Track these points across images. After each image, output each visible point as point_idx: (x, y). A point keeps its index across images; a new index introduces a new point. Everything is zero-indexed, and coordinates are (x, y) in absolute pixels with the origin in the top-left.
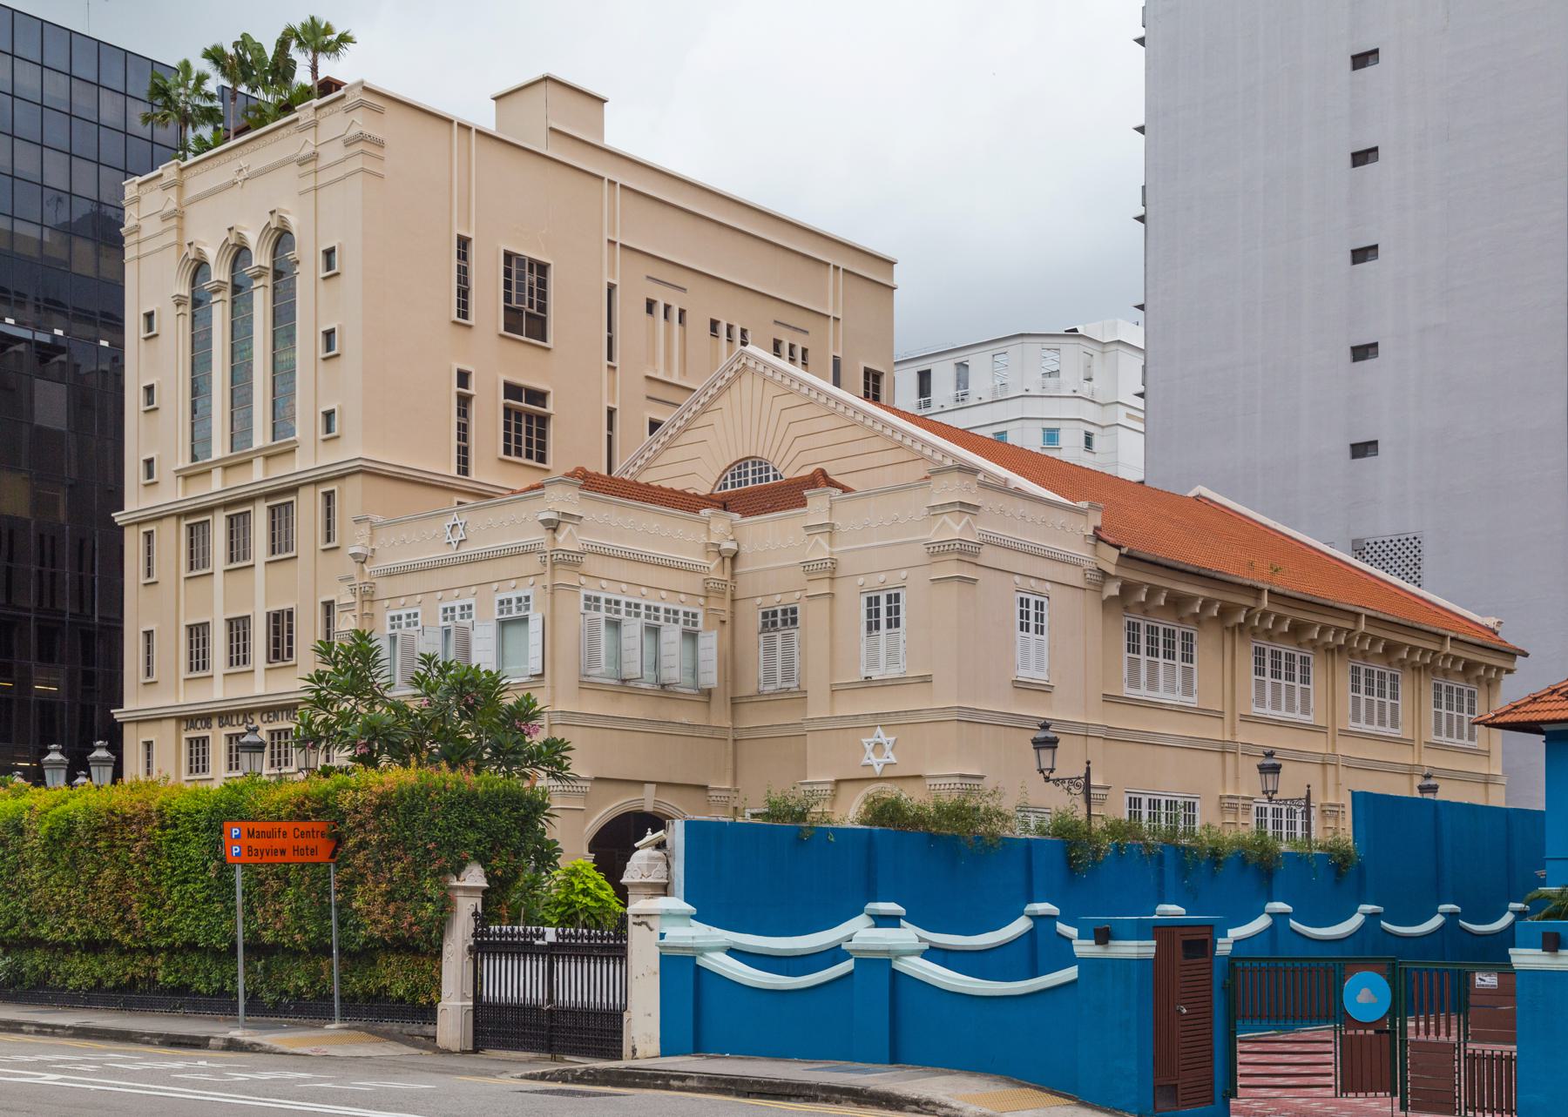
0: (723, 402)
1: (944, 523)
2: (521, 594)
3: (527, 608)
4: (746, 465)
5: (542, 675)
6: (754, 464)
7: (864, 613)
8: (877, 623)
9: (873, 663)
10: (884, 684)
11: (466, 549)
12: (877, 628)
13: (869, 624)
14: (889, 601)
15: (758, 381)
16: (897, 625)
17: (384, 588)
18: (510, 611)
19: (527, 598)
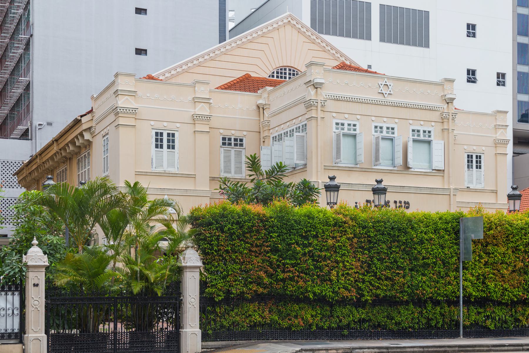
0: (275, 34)
1: (502, 132)
2: (427, 129)
3: (430, 136)
4: (285, 69)
5: (444, 171)
6: (290, 70)
7: (482, 162)
8: (472, 166)
9: (471, 182)
10: (476, 191)
11: (390, 99)
12: (472, 168)
13: (468, 165)
14: (477, 158)
15: (295, 32)
16: (480, 168)
17: (331, 105)
18: (419, 136)
19: (429, 132)
